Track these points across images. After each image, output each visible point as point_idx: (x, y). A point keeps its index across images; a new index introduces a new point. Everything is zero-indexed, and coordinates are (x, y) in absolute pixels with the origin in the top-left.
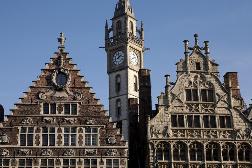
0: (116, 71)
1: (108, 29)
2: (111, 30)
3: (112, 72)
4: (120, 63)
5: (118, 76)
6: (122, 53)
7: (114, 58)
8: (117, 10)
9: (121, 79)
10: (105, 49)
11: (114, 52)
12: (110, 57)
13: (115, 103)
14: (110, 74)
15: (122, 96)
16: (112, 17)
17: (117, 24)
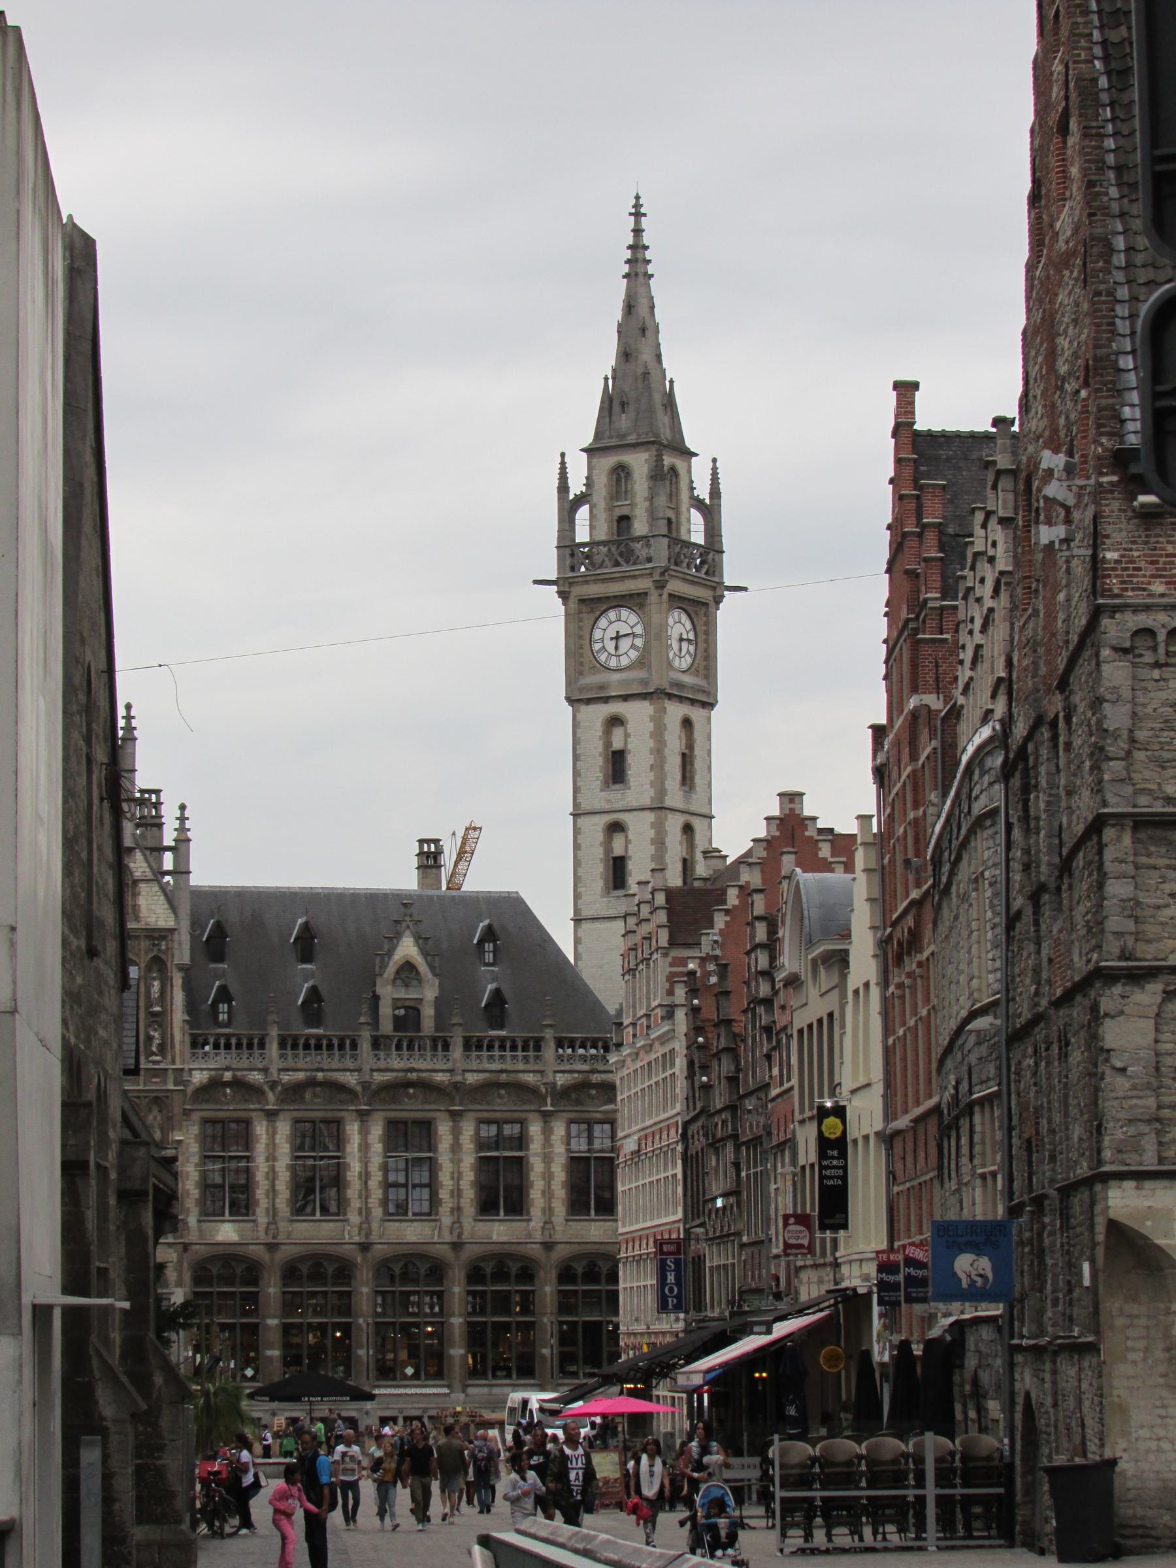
0: (606, 700)
1: (571, 497)
2: (581, 500)
3: (588, 701)
4: (625, 661)
5: (615, 721)
6: (633, 618)
7: (597, 634)
8: (611, 405)
9: (627, 735)
10: (555, 588)
11: (598, 613)
12: (580, 628)
13: (600, 837)
14: (576, 705)
15: (635, 813)
16: (588, 439)
17: (610, 480)
